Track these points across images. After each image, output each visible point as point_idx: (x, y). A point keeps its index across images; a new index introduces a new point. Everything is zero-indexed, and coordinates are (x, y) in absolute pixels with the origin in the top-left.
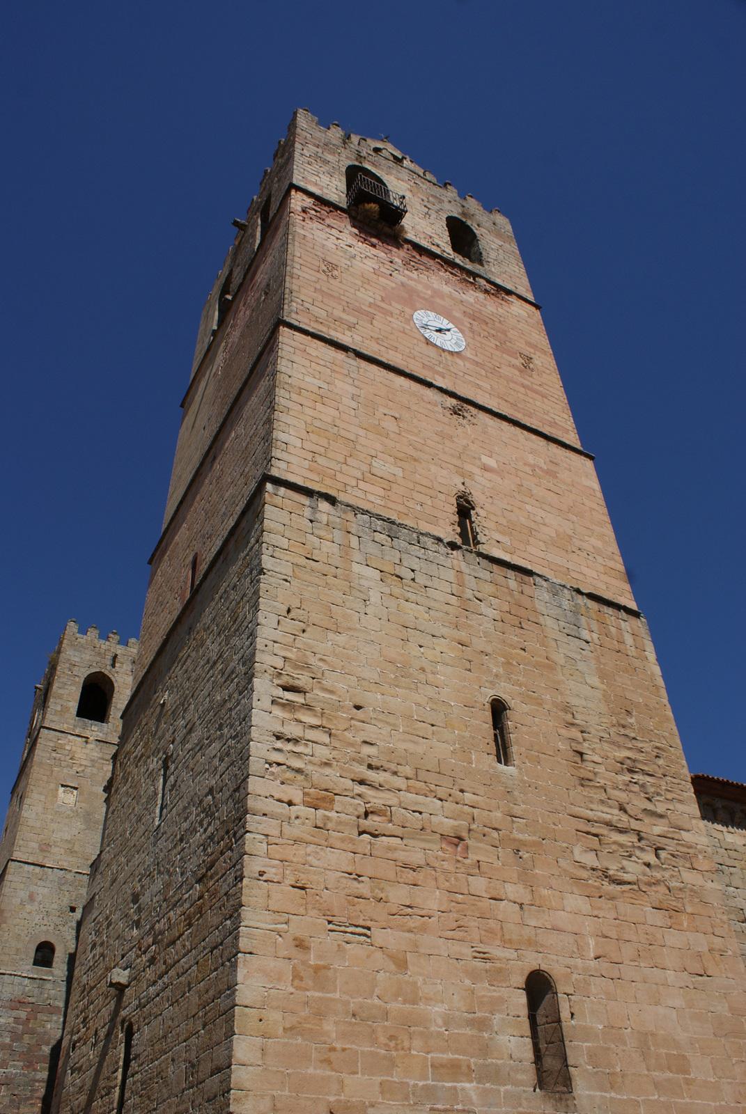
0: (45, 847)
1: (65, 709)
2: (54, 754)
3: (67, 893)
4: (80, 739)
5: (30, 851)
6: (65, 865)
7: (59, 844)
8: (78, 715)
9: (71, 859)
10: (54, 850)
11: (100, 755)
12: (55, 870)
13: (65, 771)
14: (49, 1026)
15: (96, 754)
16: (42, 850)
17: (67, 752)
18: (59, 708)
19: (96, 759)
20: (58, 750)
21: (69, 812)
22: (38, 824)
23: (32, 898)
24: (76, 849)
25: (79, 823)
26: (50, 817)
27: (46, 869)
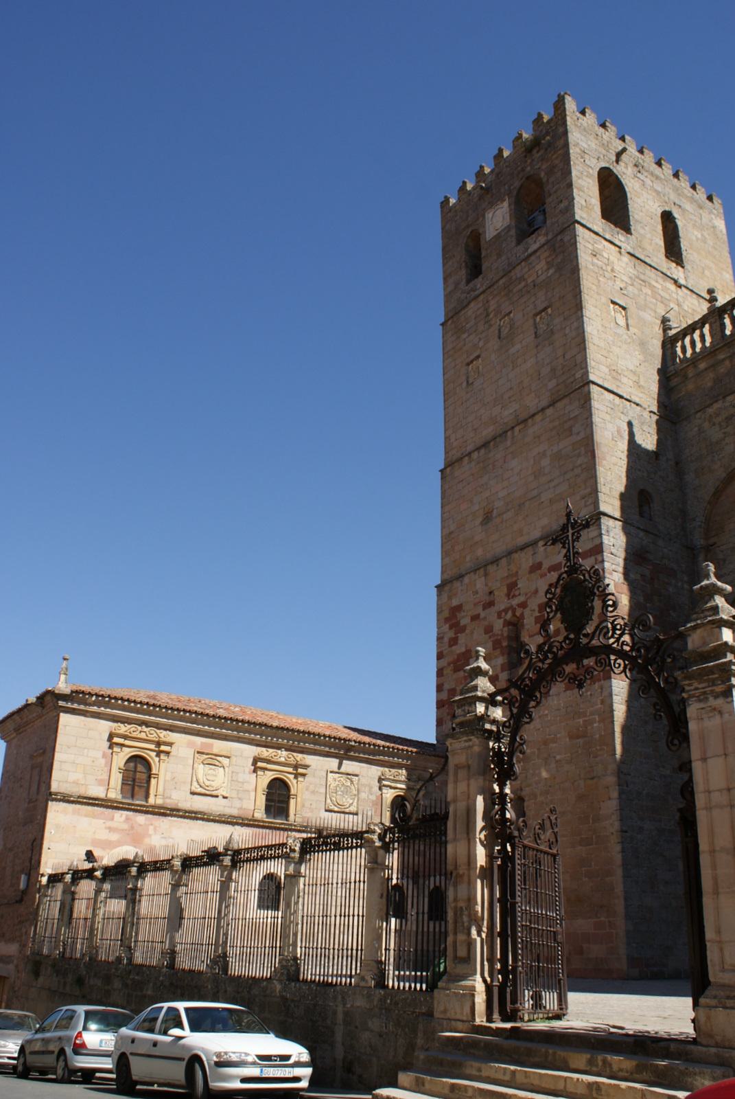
0: (615, 373)
1: (588, 207)
2: (596, 261)
3: (649, 435)
4: (612, 247)
5: (603, 375)
6: (637, 401)
7: (626, 373)
9: (641, 395)
10: (625, 380)
11: (636, 273)
12: (633, 404)
13: (610, 283)
14: (671, 590)
15: (631, 270)
17: (606, 261)
19: (633, 277)
20: (598, 256)
21: (625, 337)
22: (602, 344)
24: (642, 383)
25: (637, 353)
26: (611, 338)
27: (623, 400)
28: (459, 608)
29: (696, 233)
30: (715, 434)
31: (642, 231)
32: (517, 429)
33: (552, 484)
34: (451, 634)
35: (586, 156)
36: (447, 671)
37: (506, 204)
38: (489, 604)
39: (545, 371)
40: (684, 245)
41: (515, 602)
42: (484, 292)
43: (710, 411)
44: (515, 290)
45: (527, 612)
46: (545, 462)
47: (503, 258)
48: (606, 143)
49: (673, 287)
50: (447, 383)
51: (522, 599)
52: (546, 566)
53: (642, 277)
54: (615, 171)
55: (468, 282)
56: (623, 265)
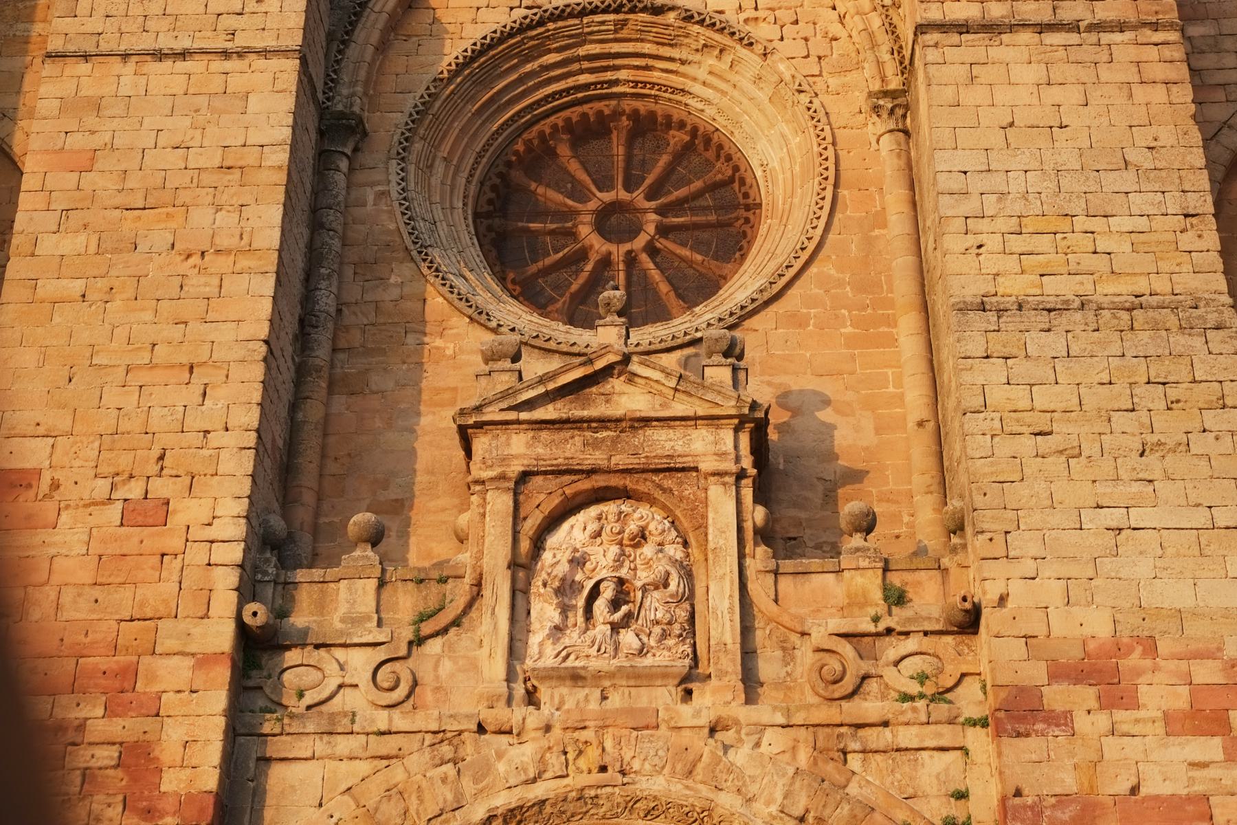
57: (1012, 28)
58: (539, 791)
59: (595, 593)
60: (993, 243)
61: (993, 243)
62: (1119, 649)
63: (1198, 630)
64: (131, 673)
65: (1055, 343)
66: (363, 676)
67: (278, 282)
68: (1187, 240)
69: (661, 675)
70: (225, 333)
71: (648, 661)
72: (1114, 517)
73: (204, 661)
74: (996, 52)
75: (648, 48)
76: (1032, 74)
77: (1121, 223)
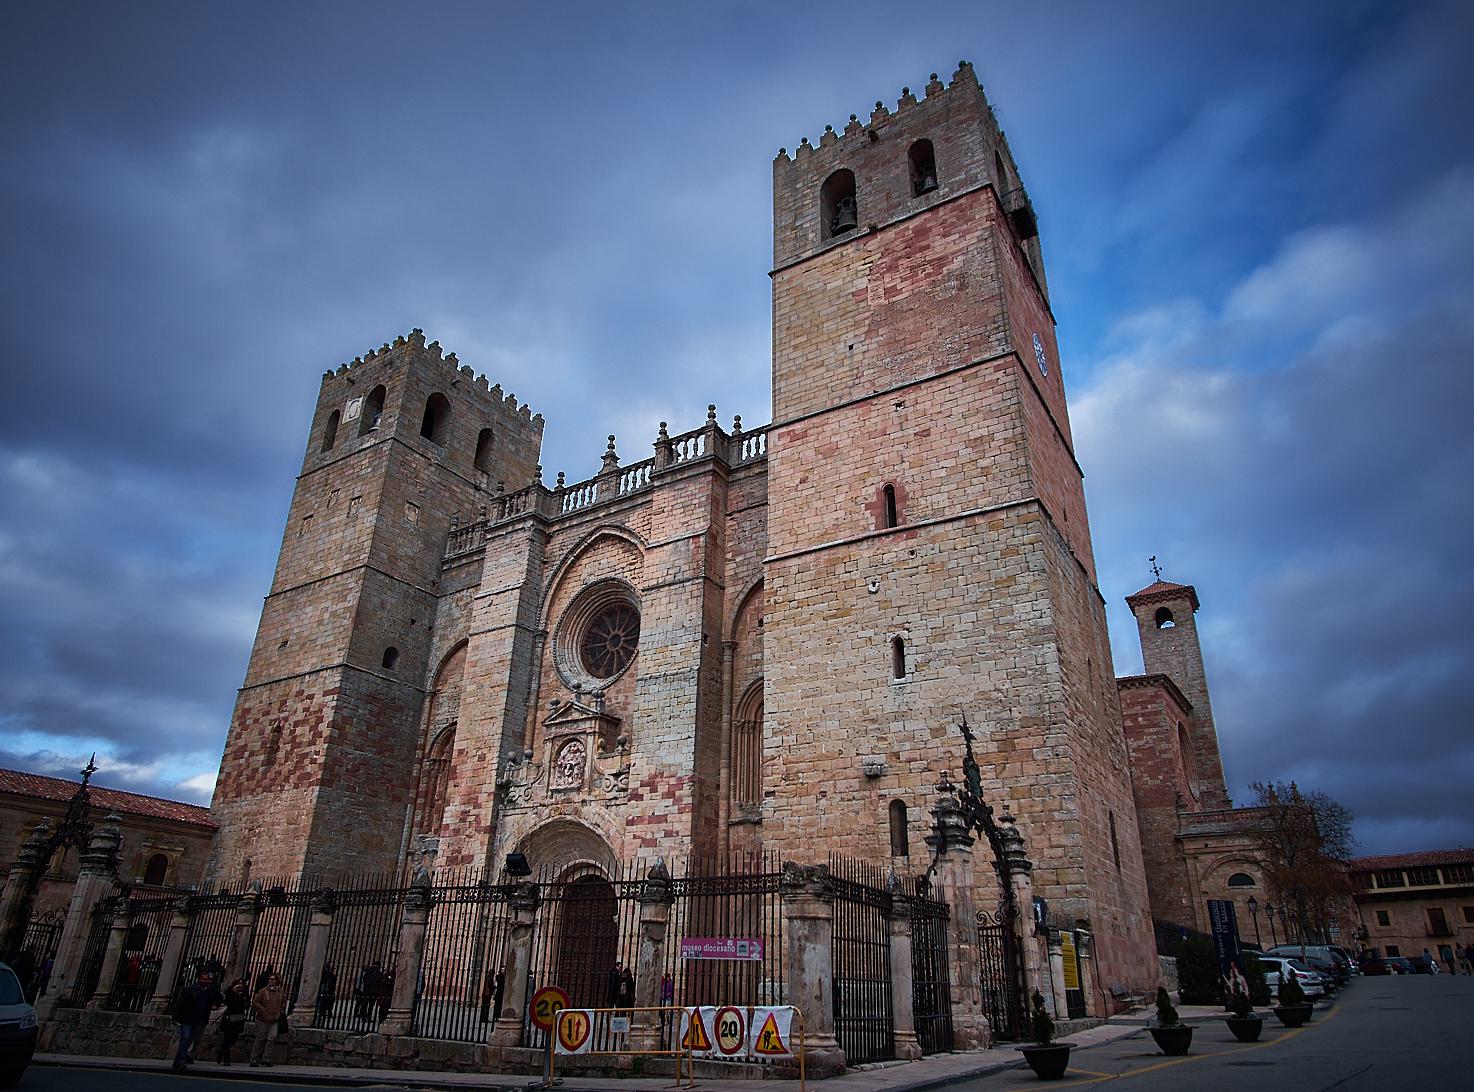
0: (393, 559)
1: (411, 426)
8: (422, 434)
10: (400, 564)
16: (390, 562)
18: (407, 423)
23: (382, 605)
28: (248, 711)
29: (510, 446)
30: (456, 613)
31: (456, 445)
32: (318, 583)
33: (326, 634)
34: (238, 730)
35: (421, 384)
36: (229, 758)
37: (361, 399)
38: (267, 713)
39: (346, 545)
40: (493, 455)
41: (282, 715)
42: (328, 465)
43: (458, 595)
44: (346, 474)
45: (287, 725)
46: (326, 616)
47: (348, 443)
48: (444, 372)
49: (472, 491)
50: (289, 528)
51: (287, 714)
52: (305, 694)
53: (444, 483)
54: (446, 395)
55: (323, 451)
56: (428, 474)
57: (663, 586)
58: (550, 820)
59: (566, 768)
60: (649, 657)
61: (649, 657)
62: (656, 776)
63: (673, 769)
64: (477, 798)
65: (656, 688)
66: (522, 793)
67: (509, 690)
68: (693, 650)
69: (572, 790)
70: (497, 708)
71: (572, 786)
72: (660, 739)
73: (489, 794)
74: (659, 595)
75: (614, 590)
76: (665, 601)
77: (679, 646)
